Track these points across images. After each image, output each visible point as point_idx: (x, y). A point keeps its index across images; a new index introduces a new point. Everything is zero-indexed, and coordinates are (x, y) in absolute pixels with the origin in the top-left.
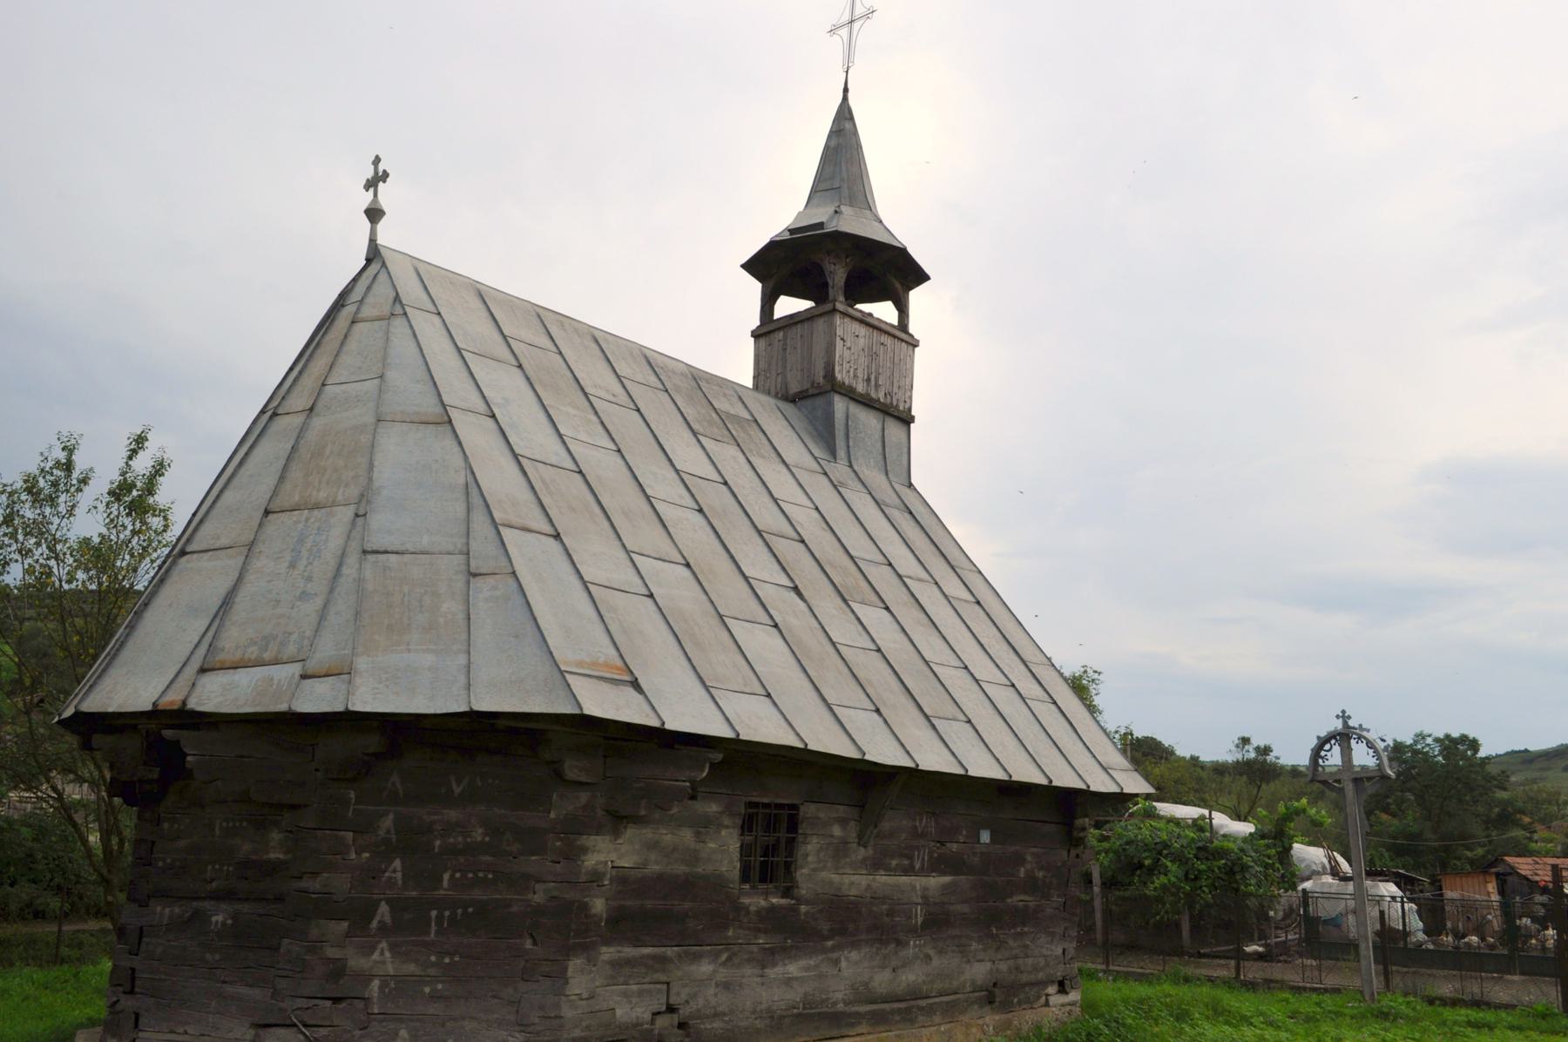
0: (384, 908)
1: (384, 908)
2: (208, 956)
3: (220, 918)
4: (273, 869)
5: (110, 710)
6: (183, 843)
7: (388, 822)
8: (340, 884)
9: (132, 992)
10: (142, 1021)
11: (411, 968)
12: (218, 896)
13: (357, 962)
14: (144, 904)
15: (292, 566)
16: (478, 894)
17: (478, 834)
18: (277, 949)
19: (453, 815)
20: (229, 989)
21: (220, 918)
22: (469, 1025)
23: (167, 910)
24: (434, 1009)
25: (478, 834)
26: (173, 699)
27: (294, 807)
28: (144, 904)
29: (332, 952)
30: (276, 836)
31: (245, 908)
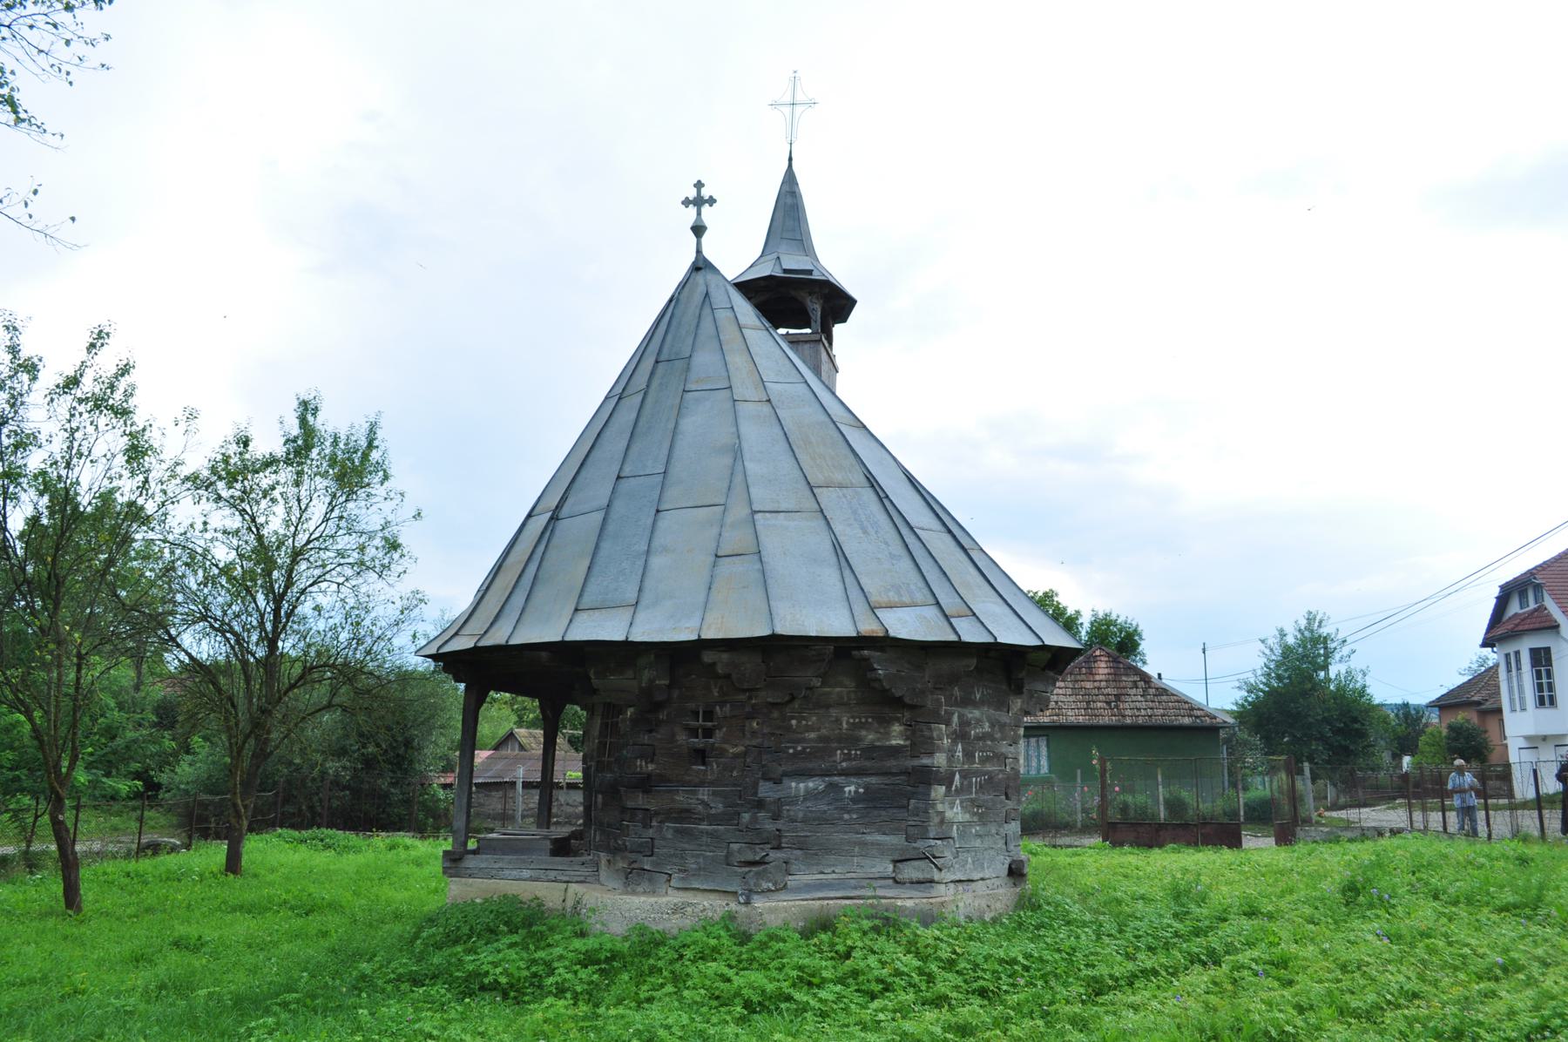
0: (957, 776)
1: (957, 776)
2: (846, 816)
3: (852, 788)
4: (895, 751)
5: (813, 634)
6: (813, 735)
7: (955, 719)
8: (940, 760)
9: (778, 848)
10: (793, 868)
11: (967, 817)
12: (845, 773)
13: (949, 814)
14: (778, 782)
15: (865, 532)
16: (989, 768)
17: (987, 728)
18: (906, 807)
19: (977, 713)
20: (868, 838)
21: (852, 788)
22: (992, 852)
23: (802, 785)
24: (978, 843)
25: (987, 728)
26: (868, 627)
27: (912, 707)
28: (778, 782)
29: (940, 807)
30: (897, 728)
31: (873, 780)
